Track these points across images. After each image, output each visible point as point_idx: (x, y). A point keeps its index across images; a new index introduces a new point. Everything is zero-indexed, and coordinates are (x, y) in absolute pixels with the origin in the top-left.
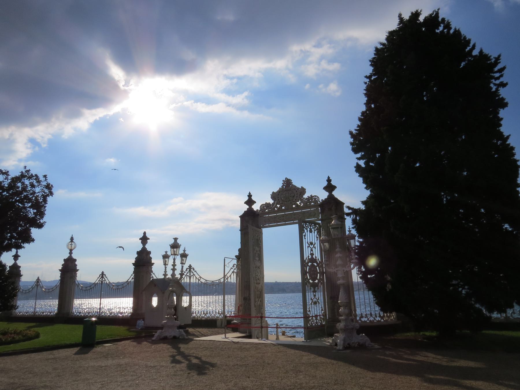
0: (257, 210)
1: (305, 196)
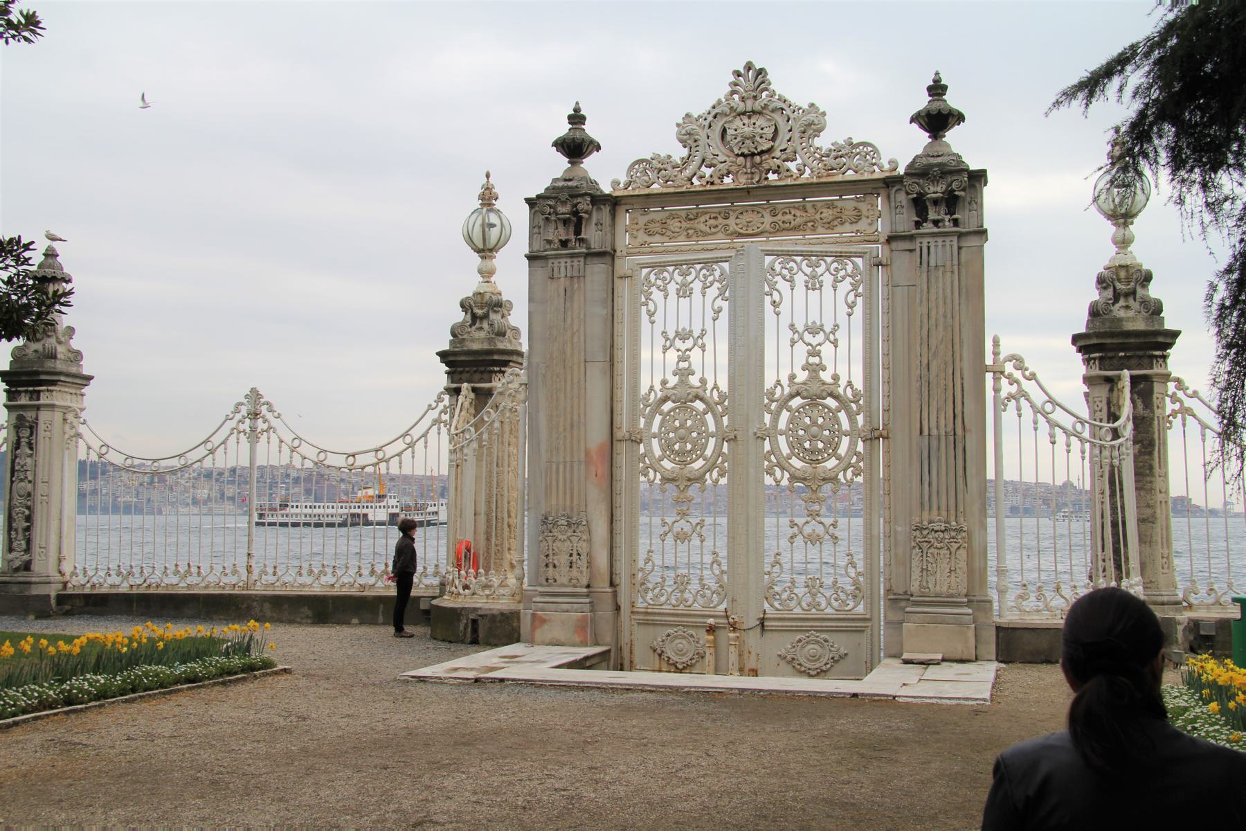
1: (824, 142)
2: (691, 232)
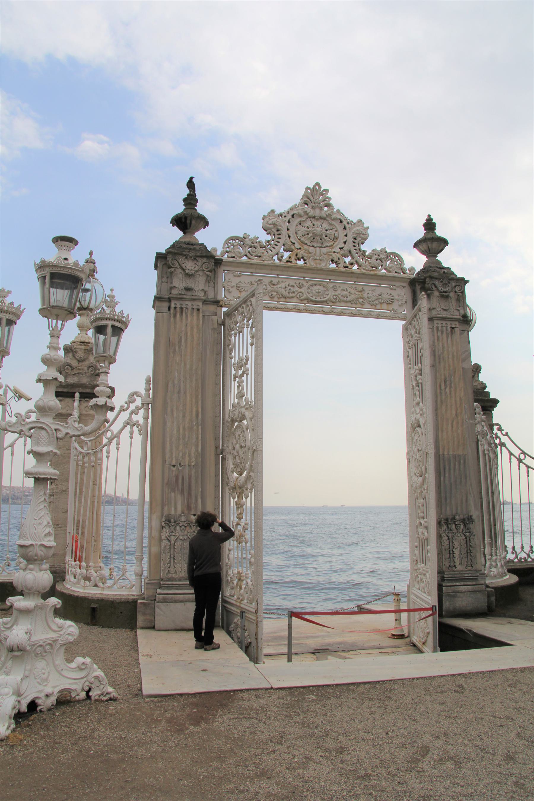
2: (274, 294)
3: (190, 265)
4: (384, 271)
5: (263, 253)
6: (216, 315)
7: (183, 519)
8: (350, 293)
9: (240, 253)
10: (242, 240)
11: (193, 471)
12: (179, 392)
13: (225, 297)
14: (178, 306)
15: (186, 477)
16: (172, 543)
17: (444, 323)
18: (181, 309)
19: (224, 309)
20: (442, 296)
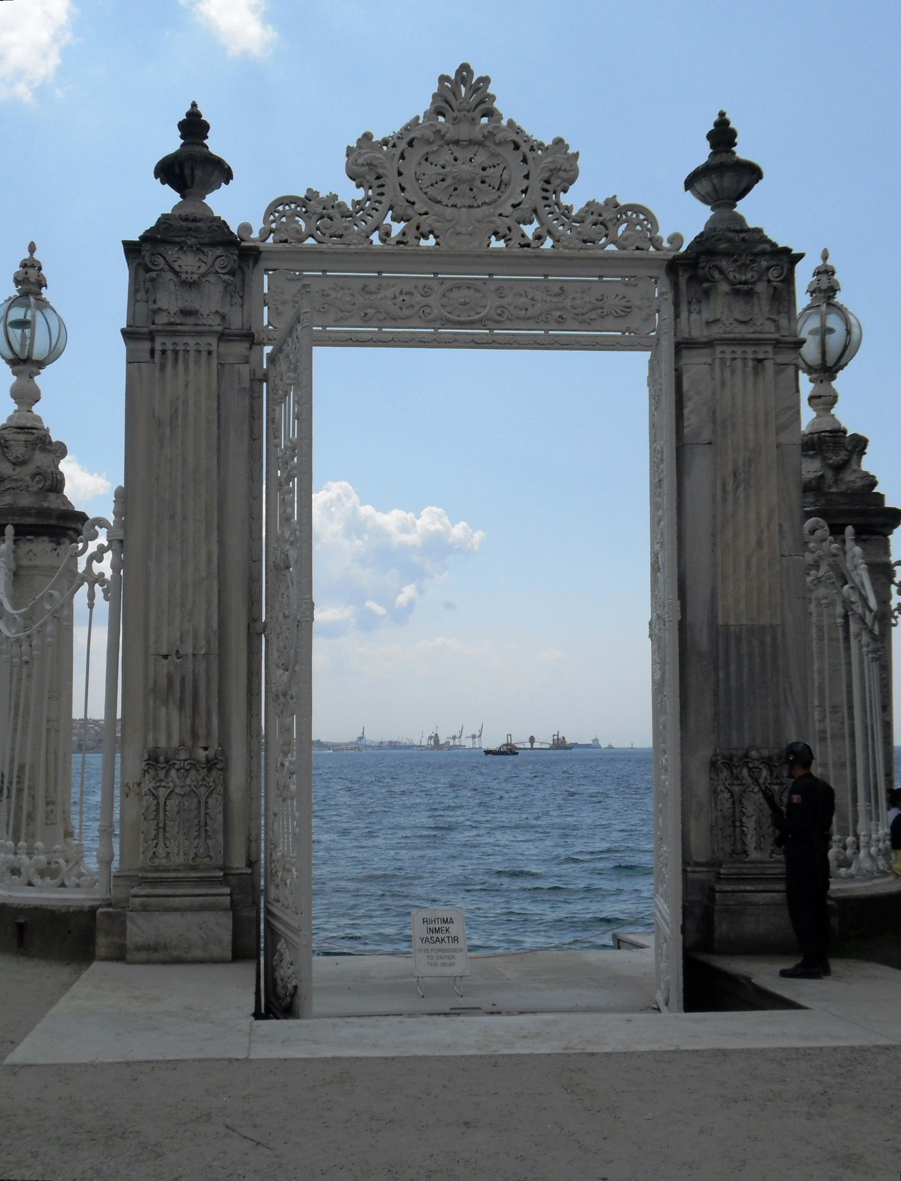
0: (246, 228)
1: (574, 199)
2: (371, 312)
3: (189, 263)
4: (611, 247)
5: (346, 228)
6: (247, 362)
7: (183, 755)
8: (533, 299)
9: (298, 231)
10: (307, 203)
11: (202, 666)
12: (172, 517)
13: (269, 324)
14: (169, 346)
15: (189, 678)
16: (162, 801)
17: (739, 350)
18: (176, 352)
19: (268, 349)
20: (736, 293)
